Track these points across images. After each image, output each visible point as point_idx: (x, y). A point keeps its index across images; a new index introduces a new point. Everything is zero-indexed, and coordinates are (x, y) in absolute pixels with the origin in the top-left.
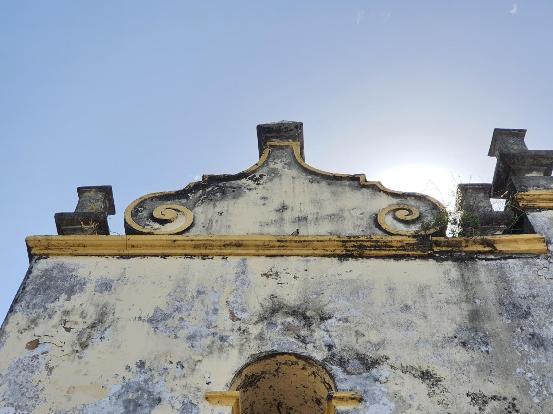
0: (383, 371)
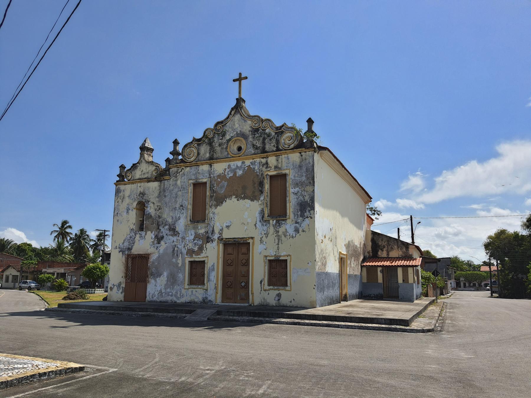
0: (150, 203)
